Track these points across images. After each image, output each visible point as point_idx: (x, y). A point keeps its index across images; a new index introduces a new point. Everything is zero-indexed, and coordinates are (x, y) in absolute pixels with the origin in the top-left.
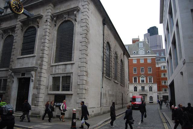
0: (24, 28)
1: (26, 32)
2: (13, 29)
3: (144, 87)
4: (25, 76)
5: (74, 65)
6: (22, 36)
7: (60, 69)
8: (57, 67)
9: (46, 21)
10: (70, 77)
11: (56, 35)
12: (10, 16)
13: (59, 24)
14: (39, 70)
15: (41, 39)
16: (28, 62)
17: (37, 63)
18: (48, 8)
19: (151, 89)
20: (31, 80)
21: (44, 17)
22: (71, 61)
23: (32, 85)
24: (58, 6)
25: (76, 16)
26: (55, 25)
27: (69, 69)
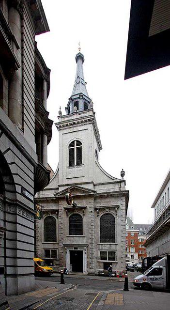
0: (68, 214)
1: (70, 217)
2: (56, 212)
3: (127, 255)
4: (78, 250)
5: (117, 246)
6: (68, 220)
7: (106, 247)
8: (106, 245)
9: (91, 212)
10: (114, 252)
11: (99, 223)
12: (47, 201)
13: (101, 215)
14: (90, 246)
15: (89, 225)
16: (77, 240)
17: (87, 242)
18: (91, 201)
19: (132, 257)
20: (84, 253)
21: (88, 208)
22: (115, 242)
23: (85, 256)
24: (98, 200)
25: (116, 212)
26: (98, 216)
27: (113, 247)
